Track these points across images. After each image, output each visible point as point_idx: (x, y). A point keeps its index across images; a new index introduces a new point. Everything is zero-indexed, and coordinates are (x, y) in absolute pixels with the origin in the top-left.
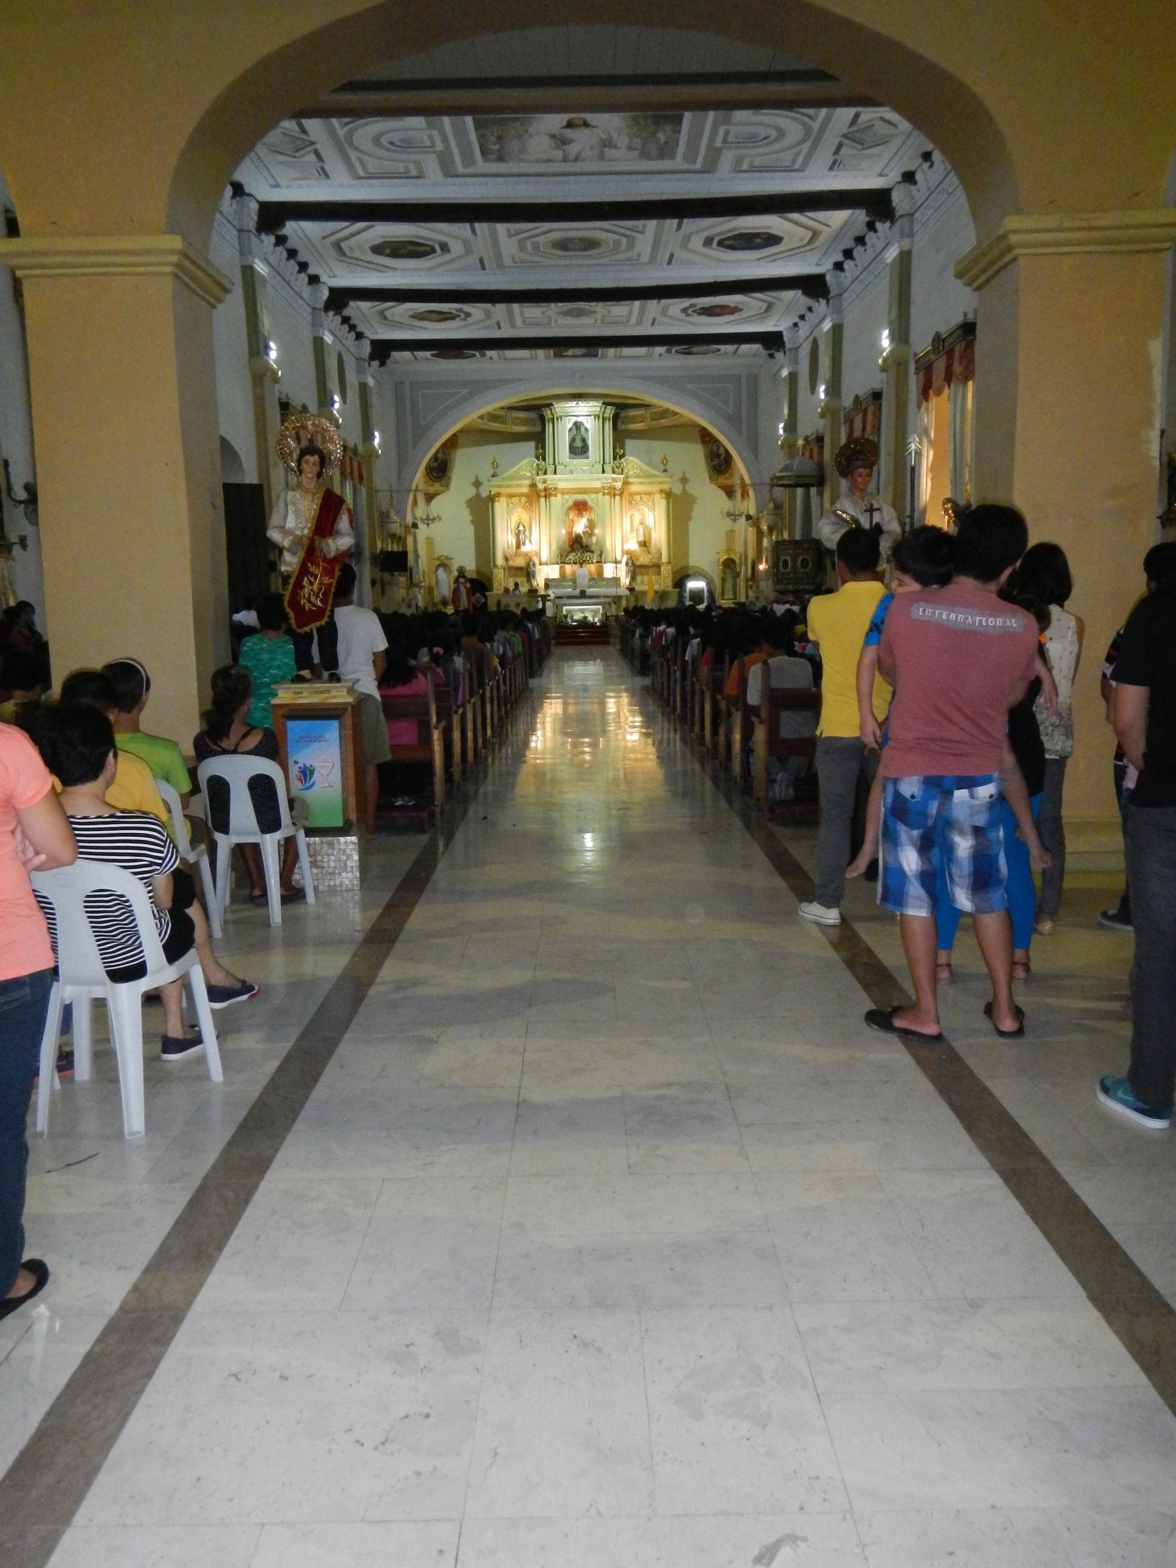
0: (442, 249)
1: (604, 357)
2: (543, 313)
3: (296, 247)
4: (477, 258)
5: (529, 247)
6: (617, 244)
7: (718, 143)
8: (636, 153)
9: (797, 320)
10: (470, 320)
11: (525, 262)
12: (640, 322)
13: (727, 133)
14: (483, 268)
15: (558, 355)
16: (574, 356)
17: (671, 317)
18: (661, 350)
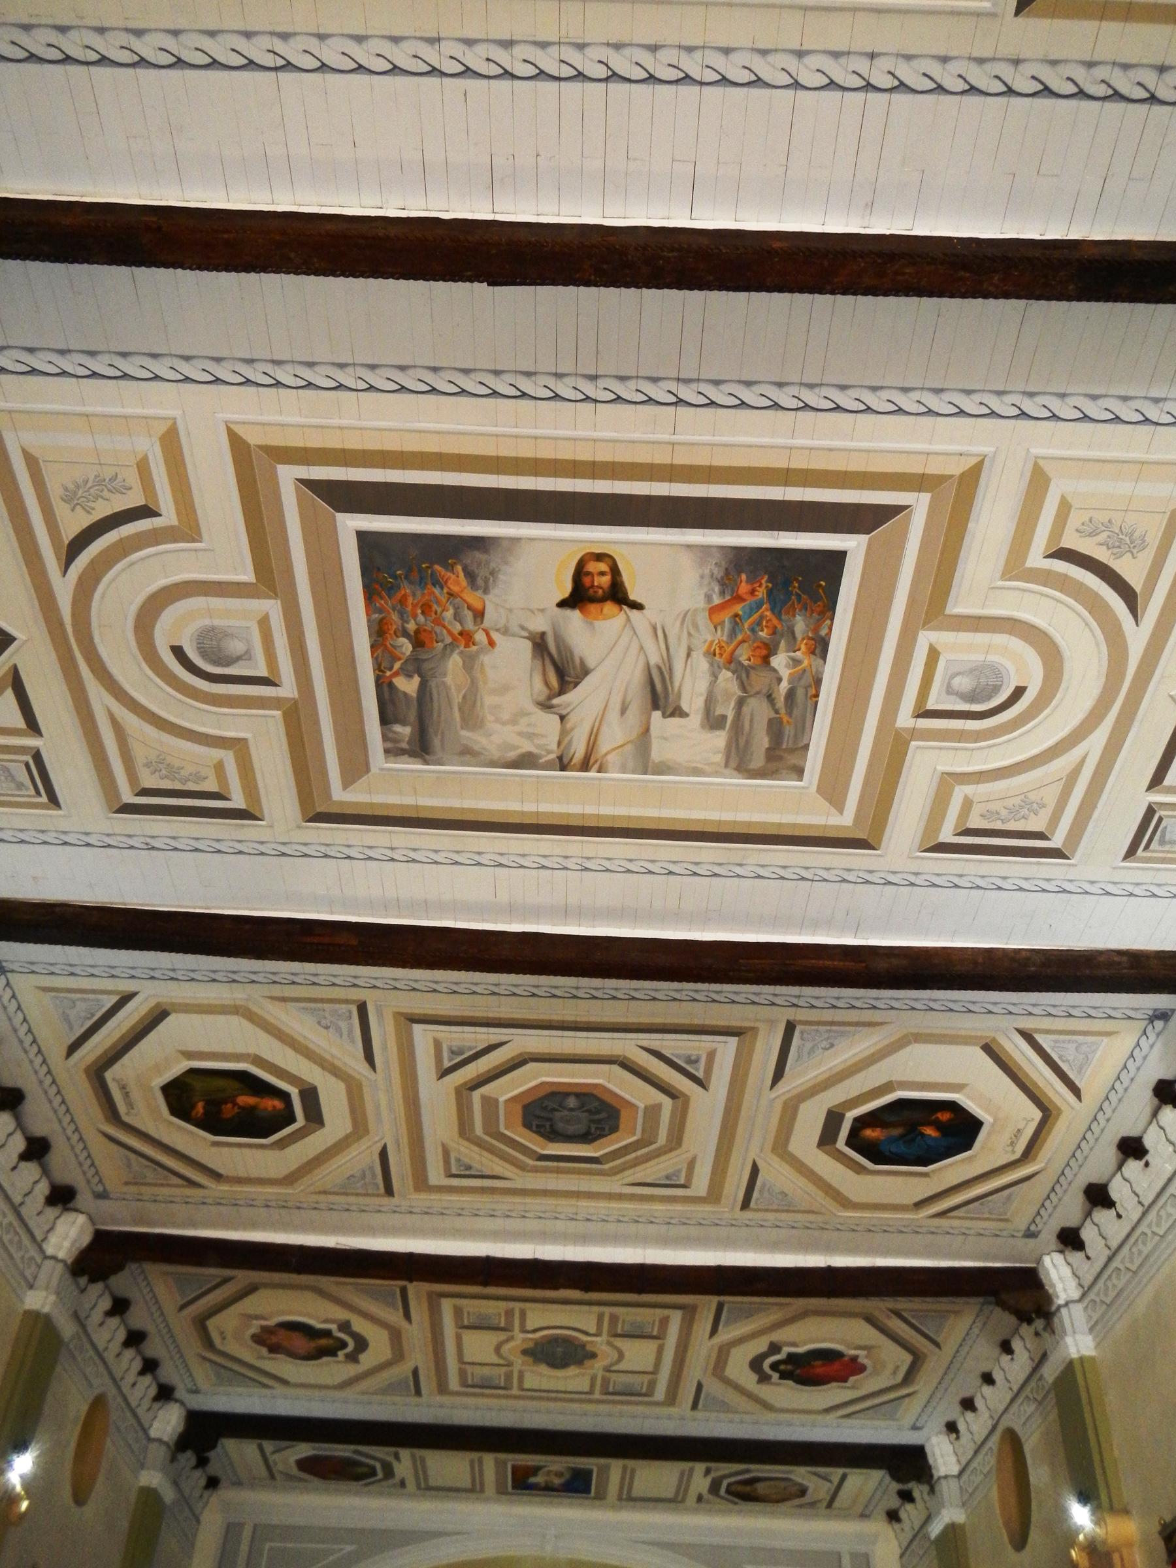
0: (308, 1117)
1: (601, 1496)
2: (497, 1350)
3: (19, 1083)
4: (379, 1147)
5: (479, 1130)
6: (653, 1111)
7: (905, 719)
8: (719, 739)
9: (954, 1412)
10: (367, 1360)
11: (468, 1173)
12: (672, 1398)
13: (933, 655)
14: (389, 1191)
15: (522, 1483)
16: (548, 1489)
17: (728, 1382)
18: (700, 1476)
